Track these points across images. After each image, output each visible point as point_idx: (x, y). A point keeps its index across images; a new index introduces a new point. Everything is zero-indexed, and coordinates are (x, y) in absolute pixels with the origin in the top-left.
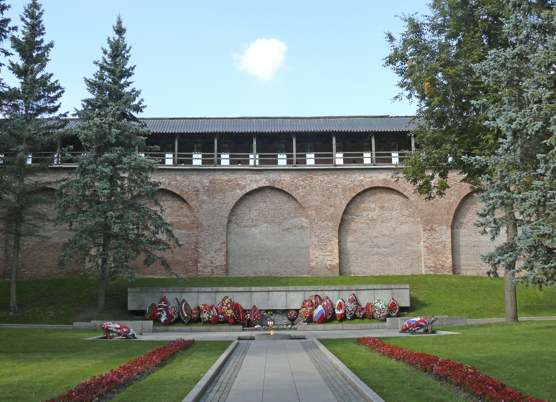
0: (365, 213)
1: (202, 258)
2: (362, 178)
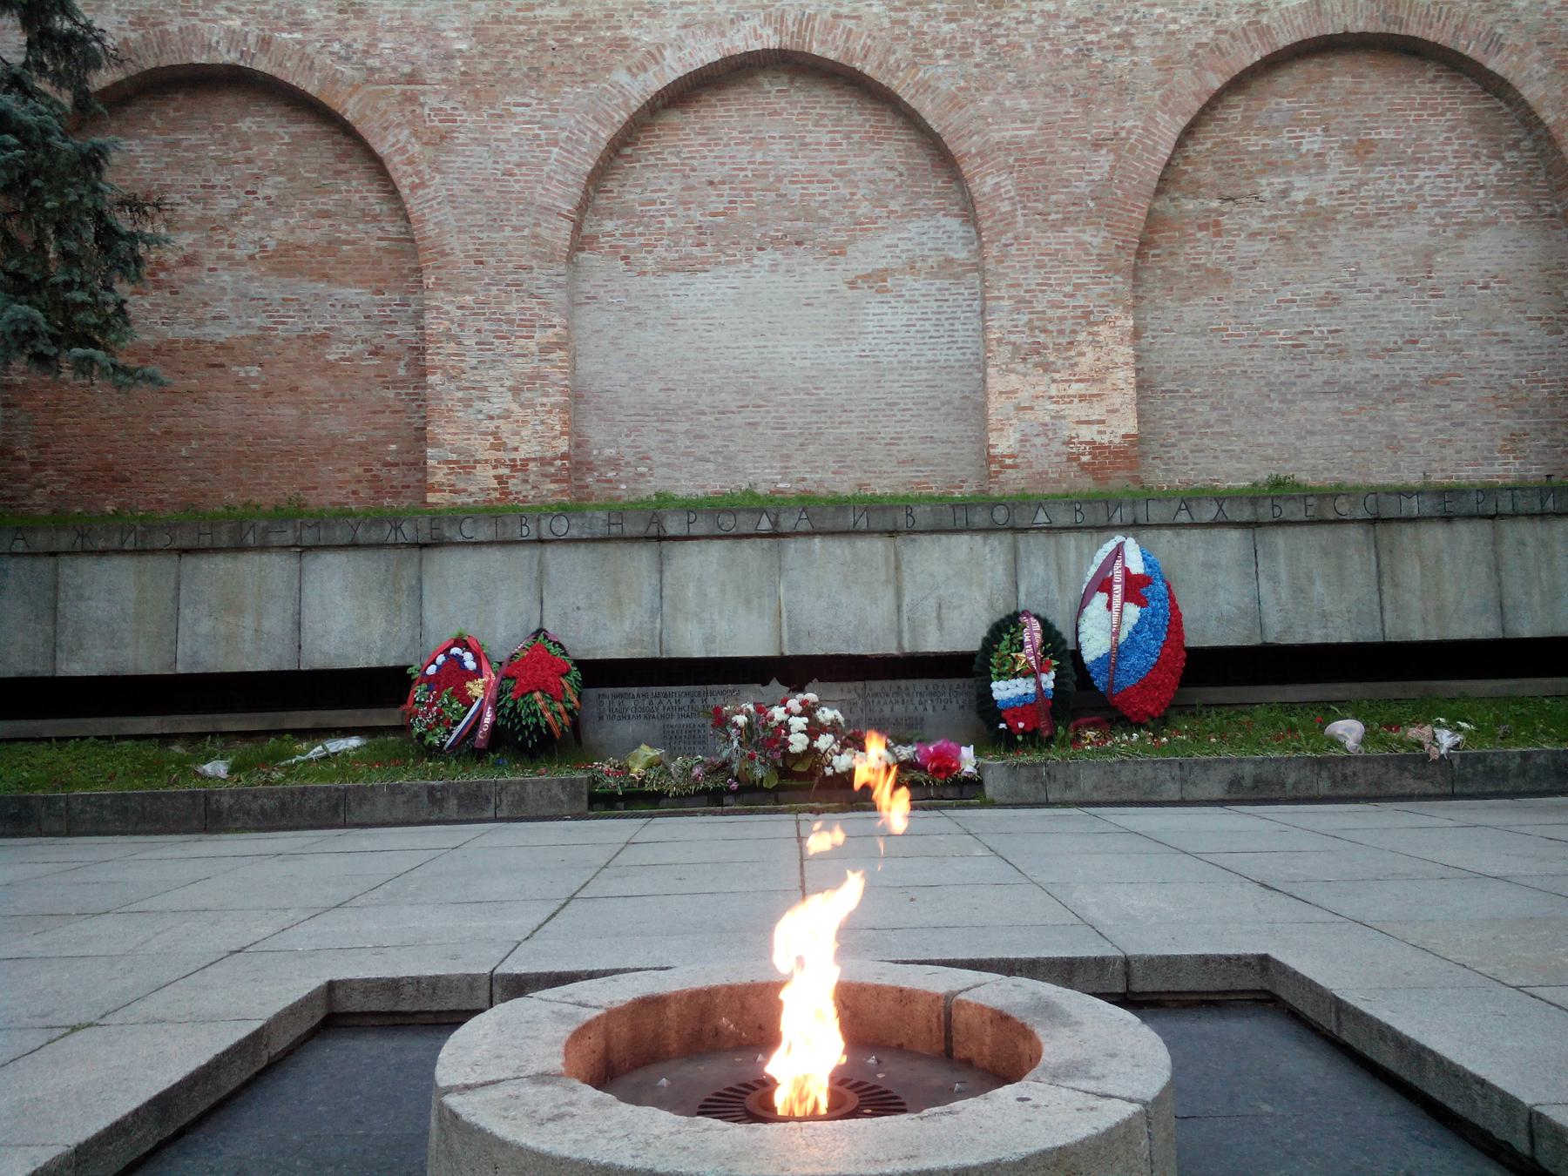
0: (1268, 185)
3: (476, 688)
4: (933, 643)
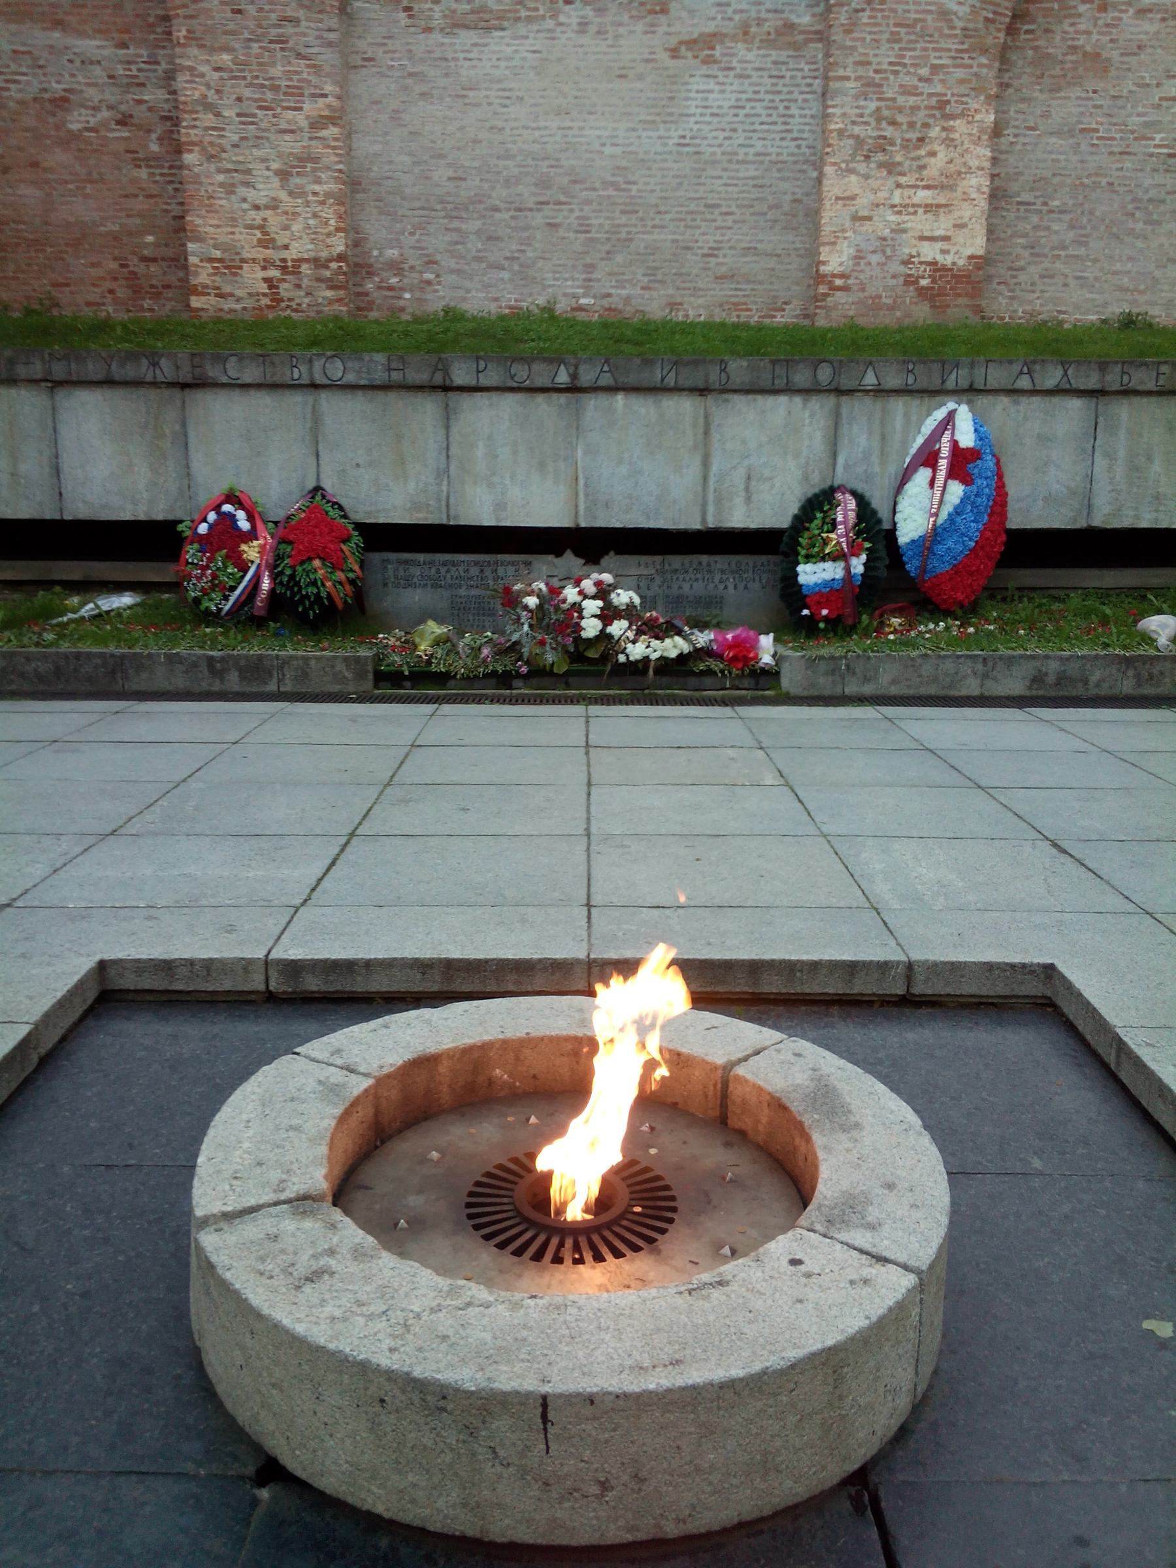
1: (211, 210)
3: (251, 552)
4: (739, 518)
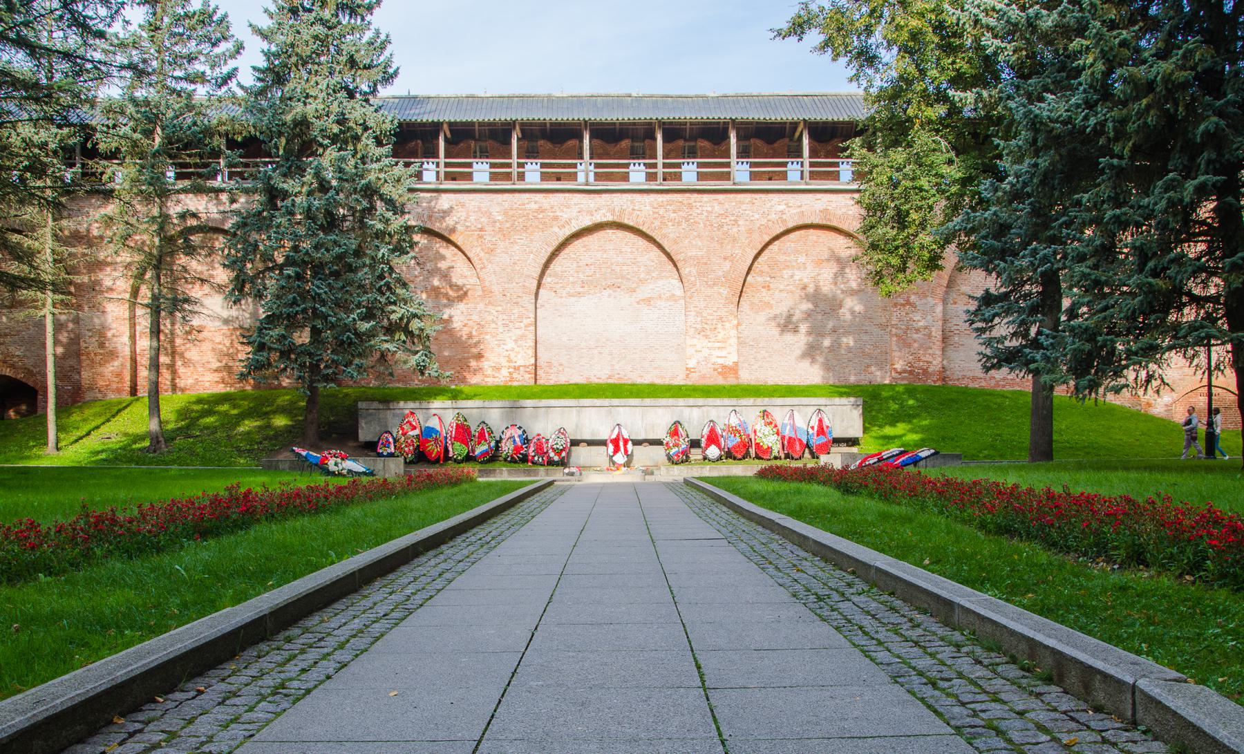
2: (782, 207)
